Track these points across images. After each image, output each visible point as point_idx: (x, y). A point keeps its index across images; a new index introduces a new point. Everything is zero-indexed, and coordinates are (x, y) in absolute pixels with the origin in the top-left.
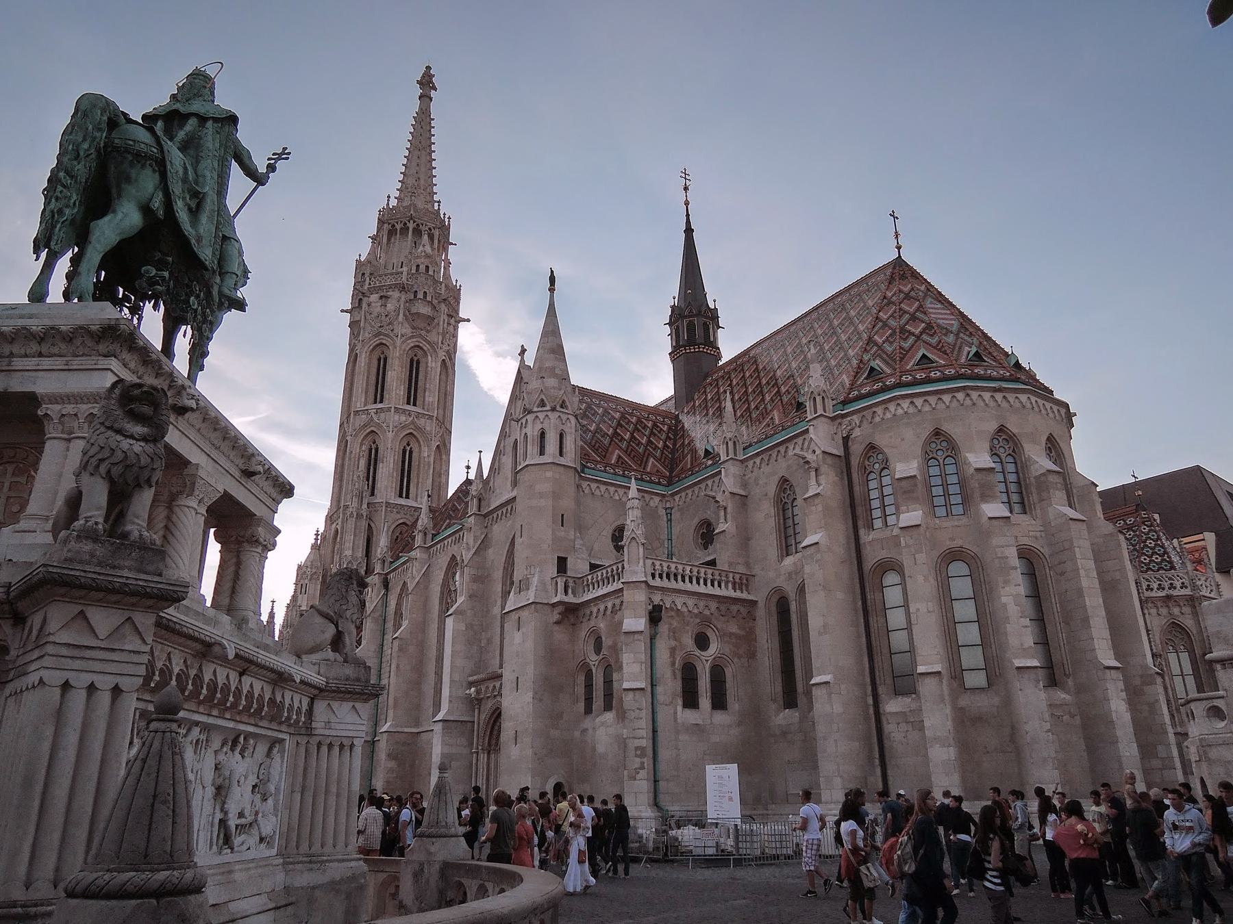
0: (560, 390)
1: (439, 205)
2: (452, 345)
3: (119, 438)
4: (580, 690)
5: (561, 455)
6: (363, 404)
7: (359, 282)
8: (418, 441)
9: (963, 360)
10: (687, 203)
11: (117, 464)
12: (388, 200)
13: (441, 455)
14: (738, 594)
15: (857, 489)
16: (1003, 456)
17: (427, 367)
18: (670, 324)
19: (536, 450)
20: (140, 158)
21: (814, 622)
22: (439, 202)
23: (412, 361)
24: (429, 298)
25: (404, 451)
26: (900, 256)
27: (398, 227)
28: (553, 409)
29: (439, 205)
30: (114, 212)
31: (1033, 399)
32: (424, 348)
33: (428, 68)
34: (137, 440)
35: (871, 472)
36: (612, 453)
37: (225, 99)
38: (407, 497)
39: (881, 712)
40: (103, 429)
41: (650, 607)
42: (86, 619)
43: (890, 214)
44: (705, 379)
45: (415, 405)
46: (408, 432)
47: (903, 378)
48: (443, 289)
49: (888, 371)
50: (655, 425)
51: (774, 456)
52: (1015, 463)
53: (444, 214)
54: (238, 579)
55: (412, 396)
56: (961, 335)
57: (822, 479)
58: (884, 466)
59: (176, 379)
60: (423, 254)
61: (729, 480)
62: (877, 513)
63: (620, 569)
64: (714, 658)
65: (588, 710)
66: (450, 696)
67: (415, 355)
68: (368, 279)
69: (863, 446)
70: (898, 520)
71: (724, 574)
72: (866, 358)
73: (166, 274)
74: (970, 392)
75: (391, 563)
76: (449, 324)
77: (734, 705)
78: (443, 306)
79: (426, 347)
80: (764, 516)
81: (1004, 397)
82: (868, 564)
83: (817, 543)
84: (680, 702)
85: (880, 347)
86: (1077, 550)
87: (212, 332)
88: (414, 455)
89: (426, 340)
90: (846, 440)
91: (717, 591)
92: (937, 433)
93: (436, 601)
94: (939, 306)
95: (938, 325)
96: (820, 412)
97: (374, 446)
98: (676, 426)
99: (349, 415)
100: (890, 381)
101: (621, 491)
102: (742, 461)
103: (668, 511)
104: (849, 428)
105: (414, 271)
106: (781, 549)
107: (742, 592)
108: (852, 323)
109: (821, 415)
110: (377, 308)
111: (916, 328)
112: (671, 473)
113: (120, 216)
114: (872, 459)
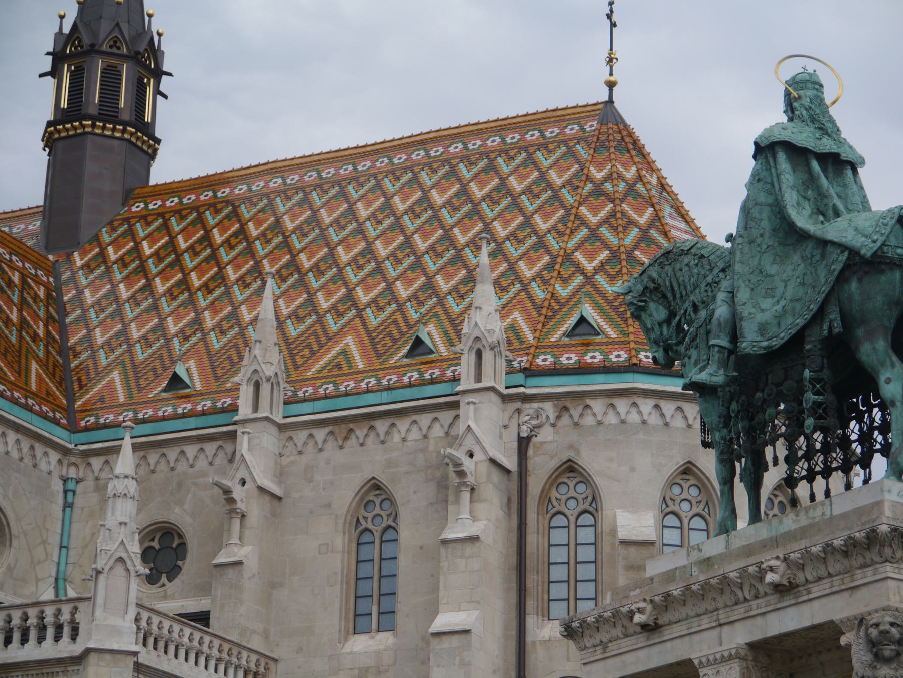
26: (610, 101)
35: (559, 512)
49: (612, 334)
58: (587, 506)
69: (554, 464)
71: (235, 652)
72: (563, 292)
83: (467, 632)
90: (523, 444)
98: (58, 290)
100: (618, 356)
102: (282, 428)
103: (71, 486)
104: (534, 422)
106: (346, 619)
114: (563, 490)
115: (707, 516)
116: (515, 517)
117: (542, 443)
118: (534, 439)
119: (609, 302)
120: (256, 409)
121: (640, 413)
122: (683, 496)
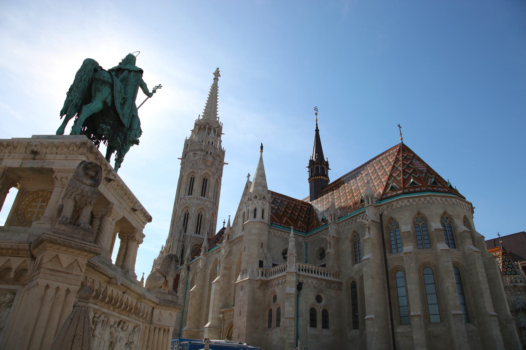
0: (263, 191)
1: (218, 119)
2: (220, 173)
3: (81, 184)
4: (267, 318)
5: (263, 218)
6: (184, 196)
7: (186, 148)
8: (204, 211)
9: (429, 184)
10: (317, 120)
11: (78, 194)
12: (199, 117)
13: (213, 217)
14: (335, 279)
15: (385, 236)
16: (446, 224)
17: (210, 182)
18: (309, 167)
19: (253, 215)
20: (104, 82)
21: (367, 292)
22: (219, 118)
23: (204, 179)
24: (212, 154)
25: (199, 215)
26: (402, 142)
27: (202, 127)
28: (260, 200)
29: (218, 119)
30: (92, 102)
31: (458, 201)
32: (210, 174)
33: (218, 69)
34: (88, 185)
35: (391, 229)
36: (284, 218)
37: (138, 64)
38: (199, 234)
39: (395, 332)
40: (75, 180)
41: (297, 283)
42: (58, 258)
43: (398, 126)
44: (323, 190)
45: (204, 196)
46: (201, 207)
47: (405, 191)
48: (218, 151)
50: (301, 207)
51: (351, 221)
52: (451, 227)
53: (220, 122)
54: (126, 254)
55: (203, 193)
56: (428, 174)
57: (371, 231)
59: (108, 167)
60: (211, 137)
61: (332, 230)
62: (394, 247)
63: (285, 267)
64: (324, 307)
65: (270, 326)
66: (212, 317)
67: (206, 177)
68: (189, 146)
70: (402, 250)
73: (109, 127)
74: (432, 197)
75: (191, 260)
76: (220, 165)
77: (332, 327)
78: (218, 158)
79: (210, 173)
80: (347, 246)
81: (446, 199)
82: (389, 269)
83: (369, 259)
84: (309, 325)
85: (395, 178)
86: (477, 264)
87: (125, 153)
88: (203, 217)
89: (210, 171)
90: (381, 215)
91: (326, 278)
92: (419, 213)
93: (209, 277)
94: (418, 162)
95: (418, 170)
96: (370, 203)
97: (187, 213)
98: (310, 208)
99: (178, 199)
101: (287, 234)
102: (337, 224)
103: (306, 243)
105: (207, 143)
106: (353, 261)
107: (336, 279)
108: (383, 168)
109: (371, 205)
110: (192, 158)
111: (409, 170)
112: (307, 228)
113: (94, 104)
115: (426, 223)
116: (381, 233)
117: (385, 215)
118: (383, 214)
119: (398, 181)
120: (331, 221)
121: (404, 203)
122: (419, 220)
